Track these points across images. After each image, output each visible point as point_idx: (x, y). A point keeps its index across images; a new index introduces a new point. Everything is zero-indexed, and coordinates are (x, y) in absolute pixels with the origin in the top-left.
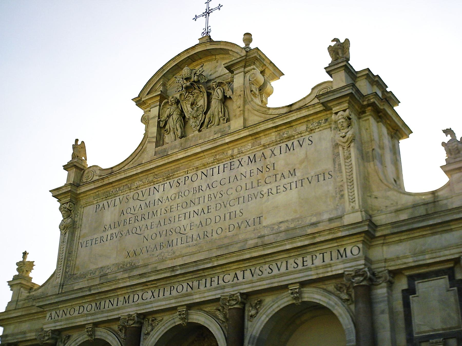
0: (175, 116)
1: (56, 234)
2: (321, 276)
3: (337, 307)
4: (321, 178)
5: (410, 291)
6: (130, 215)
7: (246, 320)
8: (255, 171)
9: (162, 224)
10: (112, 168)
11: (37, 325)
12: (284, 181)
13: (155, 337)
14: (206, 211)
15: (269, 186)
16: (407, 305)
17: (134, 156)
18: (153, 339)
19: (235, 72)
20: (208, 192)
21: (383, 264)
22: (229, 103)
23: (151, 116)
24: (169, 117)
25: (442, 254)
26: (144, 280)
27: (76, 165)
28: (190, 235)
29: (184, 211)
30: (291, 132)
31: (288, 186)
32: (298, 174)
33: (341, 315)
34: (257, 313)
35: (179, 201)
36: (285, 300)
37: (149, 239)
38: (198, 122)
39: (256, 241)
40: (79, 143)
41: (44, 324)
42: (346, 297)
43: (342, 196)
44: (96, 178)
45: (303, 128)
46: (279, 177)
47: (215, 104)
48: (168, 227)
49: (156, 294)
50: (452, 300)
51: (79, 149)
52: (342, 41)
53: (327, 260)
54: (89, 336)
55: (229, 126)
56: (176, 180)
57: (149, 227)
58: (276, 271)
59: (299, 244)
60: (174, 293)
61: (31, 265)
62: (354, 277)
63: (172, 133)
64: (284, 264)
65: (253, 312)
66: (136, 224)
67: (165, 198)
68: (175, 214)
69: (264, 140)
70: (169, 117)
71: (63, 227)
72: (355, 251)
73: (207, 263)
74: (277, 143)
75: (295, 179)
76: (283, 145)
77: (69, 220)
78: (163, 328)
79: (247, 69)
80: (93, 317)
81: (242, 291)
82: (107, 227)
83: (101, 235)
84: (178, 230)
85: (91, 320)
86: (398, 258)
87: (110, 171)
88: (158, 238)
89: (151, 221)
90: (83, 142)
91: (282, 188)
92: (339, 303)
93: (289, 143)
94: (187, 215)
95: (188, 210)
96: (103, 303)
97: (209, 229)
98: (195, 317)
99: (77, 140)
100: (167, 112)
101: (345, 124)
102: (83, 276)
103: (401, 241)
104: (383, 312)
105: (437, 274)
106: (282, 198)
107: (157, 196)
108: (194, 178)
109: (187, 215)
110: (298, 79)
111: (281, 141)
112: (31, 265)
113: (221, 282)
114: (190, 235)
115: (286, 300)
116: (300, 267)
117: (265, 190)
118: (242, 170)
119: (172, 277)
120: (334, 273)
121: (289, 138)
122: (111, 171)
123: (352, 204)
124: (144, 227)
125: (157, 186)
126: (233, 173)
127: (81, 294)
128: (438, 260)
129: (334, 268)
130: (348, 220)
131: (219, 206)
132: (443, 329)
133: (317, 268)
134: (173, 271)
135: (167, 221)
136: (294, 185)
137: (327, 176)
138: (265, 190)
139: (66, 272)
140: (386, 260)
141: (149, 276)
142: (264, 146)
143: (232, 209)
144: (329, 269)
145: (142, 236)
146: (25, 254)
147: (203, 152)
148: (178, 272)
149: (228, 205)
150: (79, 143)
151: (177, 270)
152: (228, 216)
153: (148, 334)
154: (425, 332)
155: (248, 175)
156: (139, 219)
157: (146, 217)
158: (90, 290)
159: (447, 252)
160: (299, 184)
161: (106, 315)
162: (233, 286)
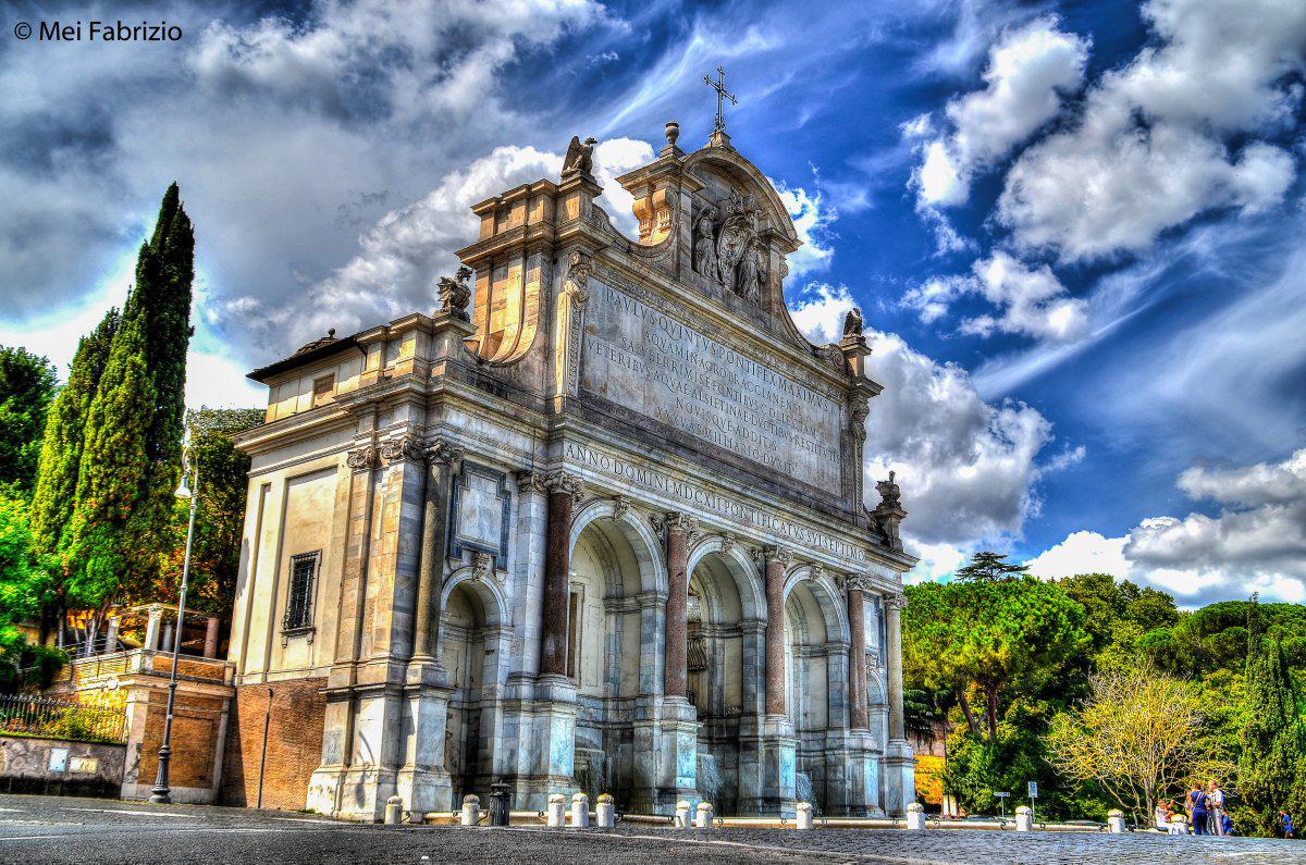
68: (710, 393)
74: (803, 384)
85: (634, 492)
158: (650, 451)
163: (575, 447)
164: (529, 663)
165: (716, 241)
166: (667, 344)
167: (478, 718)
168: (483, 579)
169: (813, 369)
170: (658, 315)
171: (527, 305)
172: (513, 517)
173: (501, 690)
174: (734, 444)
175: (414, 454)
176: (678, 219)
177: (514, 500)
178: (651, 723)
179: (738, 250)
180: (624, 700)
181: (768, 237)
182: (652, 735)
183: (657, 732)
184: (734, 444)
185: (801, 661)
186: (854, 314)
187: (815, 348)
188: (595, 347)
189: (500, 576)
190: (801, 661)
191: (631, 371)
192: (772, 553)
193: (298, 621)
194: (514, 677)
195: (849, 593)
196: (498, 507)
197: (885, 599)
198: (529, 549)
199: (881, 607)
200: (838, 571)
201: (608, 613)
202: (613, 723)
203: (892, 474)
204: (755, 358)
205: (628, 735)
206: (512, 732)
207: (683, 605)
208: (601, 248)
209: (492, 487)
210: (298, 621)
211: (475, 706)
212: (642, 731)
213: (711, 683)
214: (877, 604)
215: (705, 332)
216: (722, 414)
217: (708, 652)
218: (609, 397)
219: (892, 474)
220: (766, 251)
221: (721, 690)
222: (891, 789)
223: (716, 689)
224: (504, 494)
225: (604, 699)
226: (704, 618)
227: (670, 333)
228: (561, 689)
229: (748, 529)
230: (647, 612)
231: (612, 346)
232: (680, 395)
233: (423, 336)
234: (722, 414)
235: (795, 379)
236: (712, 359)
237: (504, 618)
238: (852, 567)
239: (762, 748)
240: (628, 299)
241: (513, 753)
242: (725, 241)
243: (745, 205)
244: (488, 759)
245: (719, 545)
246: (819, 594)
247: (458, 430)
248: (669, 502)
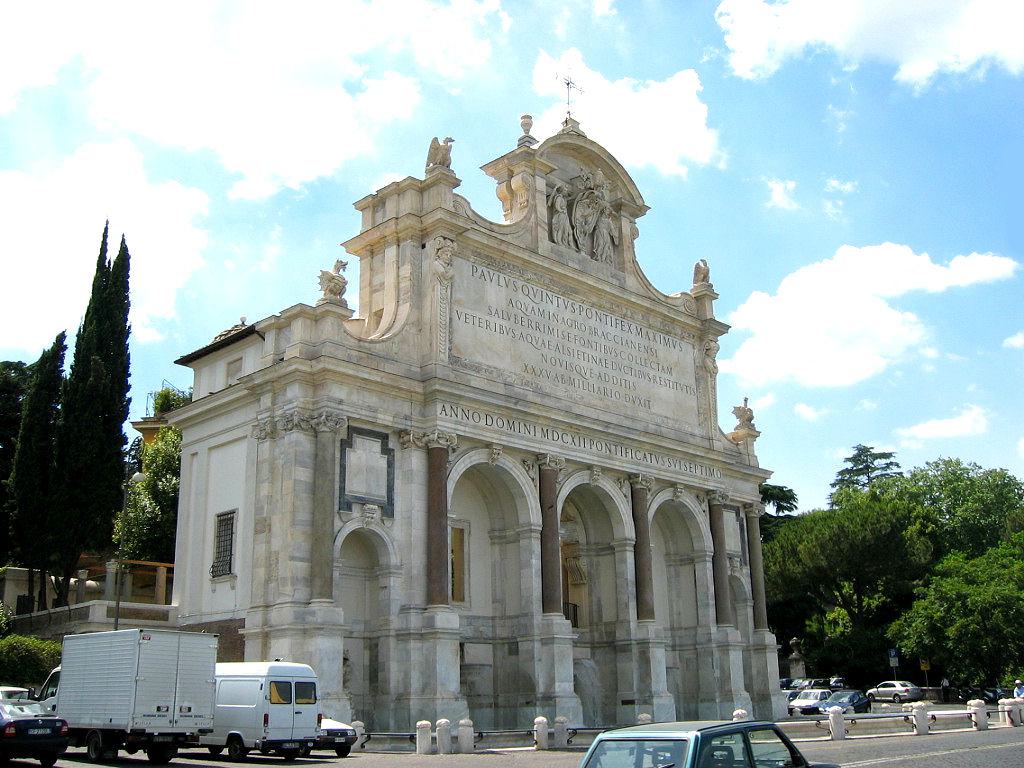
10: (491, 223)
29: (582, 349)
55: (624, 279)
63: (560, 232)
68: (572, 346)
80: (508, 439)
85: (505, 440)
96: (516, 424)
121: (668, 333)
126: (626, 335)
156: (533, 324)
158: (516, 404)
163: (448, 409)
164: (419, 598)
165: (570, 215)
166: (530, 310)
167: (377, 645)
168: (373, 527)
169: (665, 316)
170: (520, 284)
171: (402, 285)
172: (398, 473)
173: (395, 623)
175: (303, 425)
176: (534, 197)
177: (398, 455)
178: (531, 638)
179: (592, 221)
180: (510, 617)
181: (618, 207)
182: (533, 647)
183: (537, 645)
185: (672, 569)
186: (702, 264)
188: (463, 317)
189: (388, 523)
190: (672, 569)
191: (498, 335)
192: (636, 480)
193: (223, 567)
194: (405, 609)
195: (710, 507)
196: (383, 462)
197: (745, 508)
198: (411, 498)
199: (742, 515)
200: (701, 489)
201: (493, 544)
202: (502, 639)
203: (746, 400)
205: (514, 650)
206: (405, 660)
207: (556, 533)
208: (461, 232)
209: (376, 446)
210: (223, 567)
211: (375, 635)
212: (523, 646)
213: (590, 595)
214: (738, 514)
215: (563, 294)
216: (584, 364)
217: (584, 569)
219: (746, 400)
220: (617, 219)
221: (599, 600)
222: (758, 672)
223: (595, 599)
224: (386, 451)
225: (493, 618)
226: (582, 539)
227: (532, 297)
228: (447, 618)
229: (611, 462)
230: (523, 543)
232: (545, 351)
233: (309, 322)
234: (584, 364)
236: (572, 316)
237: (394, 560)
238: (710, 486)
239: (635, 650)
240: (491, 272)
241: (407, 675)
242: (578, 212)
243: (594, 179)
244: (387, 681)
245: (587, 477)
246: (683, 511)
247: (341, 402)
248: (537, 445)
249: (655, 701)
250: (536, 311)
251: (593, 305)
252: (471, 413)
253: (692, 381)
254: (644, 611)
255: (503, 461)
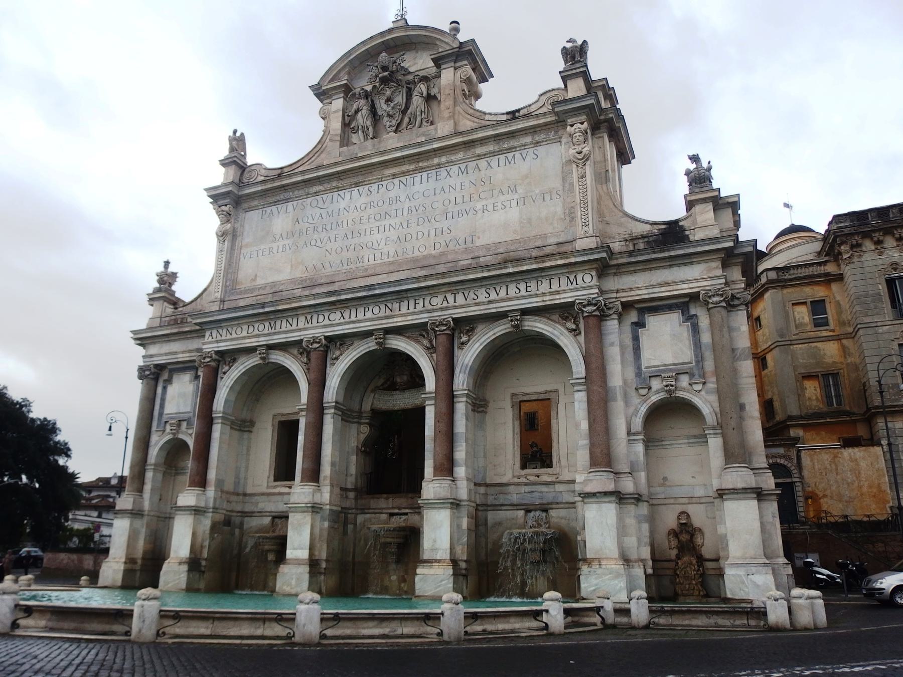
0: (365, 111)
1: (213, 243)
2: (548, 303)
3: (562, 337)
4: (547, 197)
5: (640, 324)
6: (307, 225)
7: (456, 348)
8: (467, 184)
9: (350, 237)
10: (282, 168)
11: (194, 344)
12: (502, 198)
13: (345, 362)
14: (405, 225)
15: (484, 202)
16: (636, 339)
17: (311, 156)
18: (343, 365)
19: (443, 67)
20: (407, 204)
21: (614, 295)
22: (434, 105)
23: (333, 110)
24: (357, 112)
25: (679, 287)
26: (333, 299)
27: (235, 159)
28: (385, 250)
29: (378, 224)
30: (514, 143)
31: (507, 204)
32: (520, 190)
33: (566, 346)
34: (469, 341)
35: (371, 211)
36: (501, 329)
37: (333, 253)
38: (394, 123)
39: (469, 262)
40: (238, 134)
41: (204, 344)
42: (574, 327)
43: (573, 219)
44: (261, 178)
45: (528, 139)
46: (496, 192)
47: (417, 101)
48: (356, 241)
49: (346, 315)
50: (685, 335)
51: (238, 142)
52: (580, 42)
53: (555, 287)
54: (262, 358)
55: (436, 129)
56: (367, 187)
57: (333, 240)
58: (493, 296)
59: (525, 268)
60: (369, 314)
61: (174, 276)
62: (585, 306)
63: (360, 132)
64: (504, 288)
65: (464, 339)
66: (315, 236)
67: (353, 207)
69: (479, 150)
70: (357, 112)
71: (222, 235)
72: (588, 278)
73: (411, 283)
74: (493, 154)
75: (516, 196)
76: (502, 157)
77: (229, 226)
78: (354, 353)
79: (458, 64)
81: (454, 316)
82: (277, 237)
83: (270, 245)
84: (370, 245)
85: (263, 341)
86: (632, 289)
87: (279, 171)
88: (345, 253)
89: (335, 232)
90: (242, 134)
91: (499, 206)
92: (566, 332)
93: (510, 155)
94: (382, 228)
95: (383, 223)
96: (278, 323)
97: (409, 247)
98: (394, 342)
99: (235, 132)
100: (355, 107)
101: (582, 139)
102: (246, 291)
103: (635, 272)
104: (612, 344)
105: (670, 308)
106: (499, 217)
107: (342, 204)
108: (390, 187)
109: (382, 228)
110: (519, 80)
111: (500, 152)
112: (174, 276)
113: (427, 302)
114: (385, 250)
115: (503, 327)
116: (523, 293)
117: (479, 206)
118: (451, 181)
119: (371, 298)
120: (562, 301)
121: (510, 149)
122: (281, 173)
123: (587, 228)
124: (325, 239)
125: (341, 193)
127: (251, 312)
128: (675, 293)
129: (562, 296)
130: (580, 245)
131: (421, 220)
132: (675, 364)
133: (543, 294)
134: (370, 290)
135: (356, 234)
136: (514, 203)
137: (554, 197)
138: (479, 206)
139: (226, 286)
140: (618, 291)
141: (339, 295)
142: (479, 156)
143: (438, 225)
144: (557, 297)
145: (324, 249)
146: (167, 263)
147: (403, 157)
148: (377, 292)
149: (433, 220)
150: (238, 134)
151: (375, 289)
152: (432, 233)
153: (337, 359)
154: (654, 367)
155: (458, 187)
156: (320, 229)
157: (329, 228)
158: (263, 307)
159: (685, 286)
160: (521, 203)
161: (284, 336)
162: (442, 309)
168: (180, 436)
170: (309, 200)
174: (391, 254)
184: (391, 254)
186: (569, 45)
187: (513, 113)
203: (695, 159)
204: (421, 170)
215: (357, 185)
216: (377, 236)
218: (260, 282)
231: (262, 247)
235: (480, 157)
236: (369, 199)
238: (567, 297)
249: (419, 571)
250: (324, 213)
251: (394, 176)
252: (235, 328)
253: (557, 184)
254: (447, 468)
255: (275, 357)
